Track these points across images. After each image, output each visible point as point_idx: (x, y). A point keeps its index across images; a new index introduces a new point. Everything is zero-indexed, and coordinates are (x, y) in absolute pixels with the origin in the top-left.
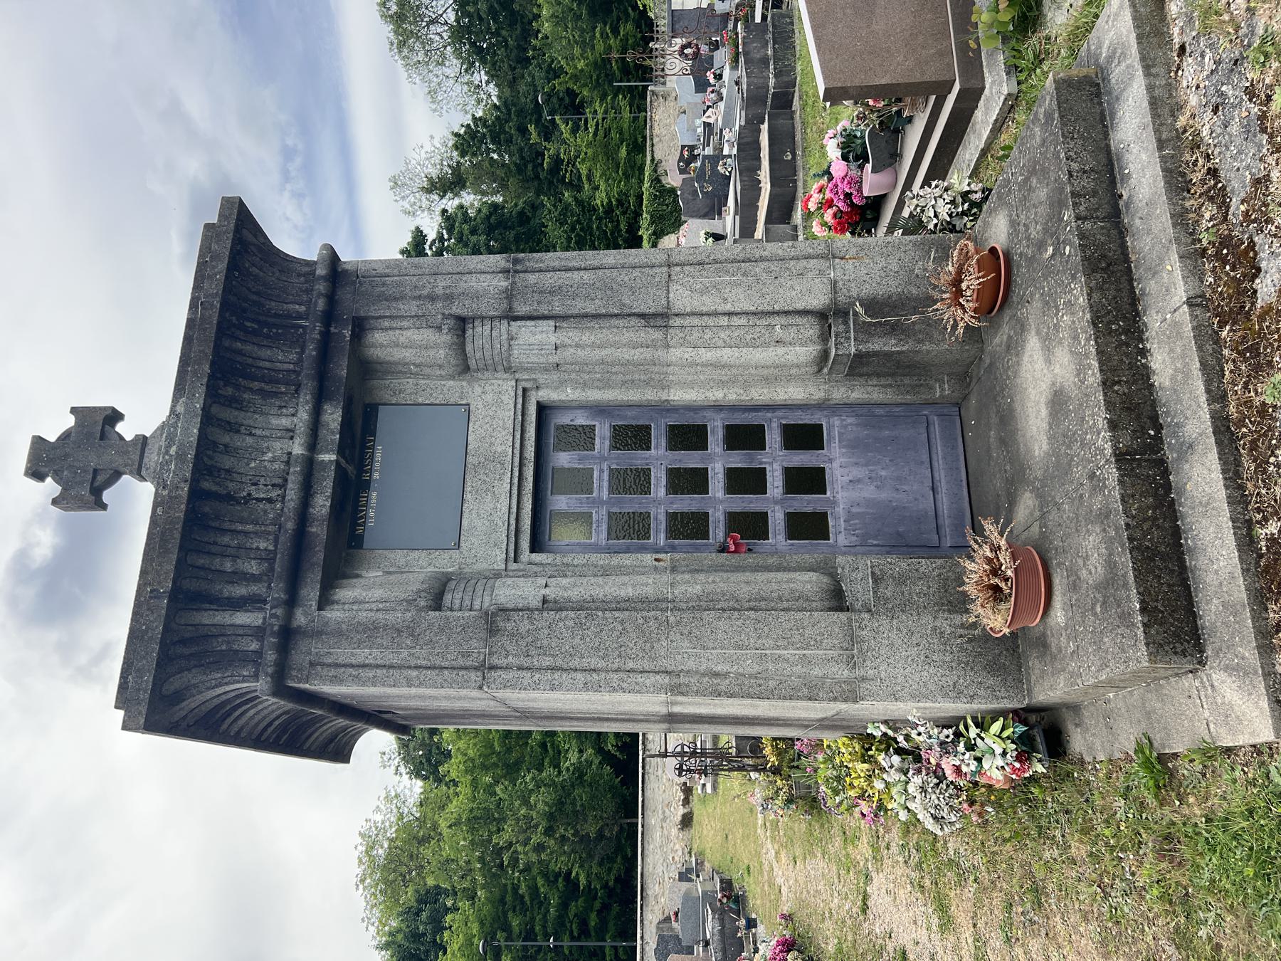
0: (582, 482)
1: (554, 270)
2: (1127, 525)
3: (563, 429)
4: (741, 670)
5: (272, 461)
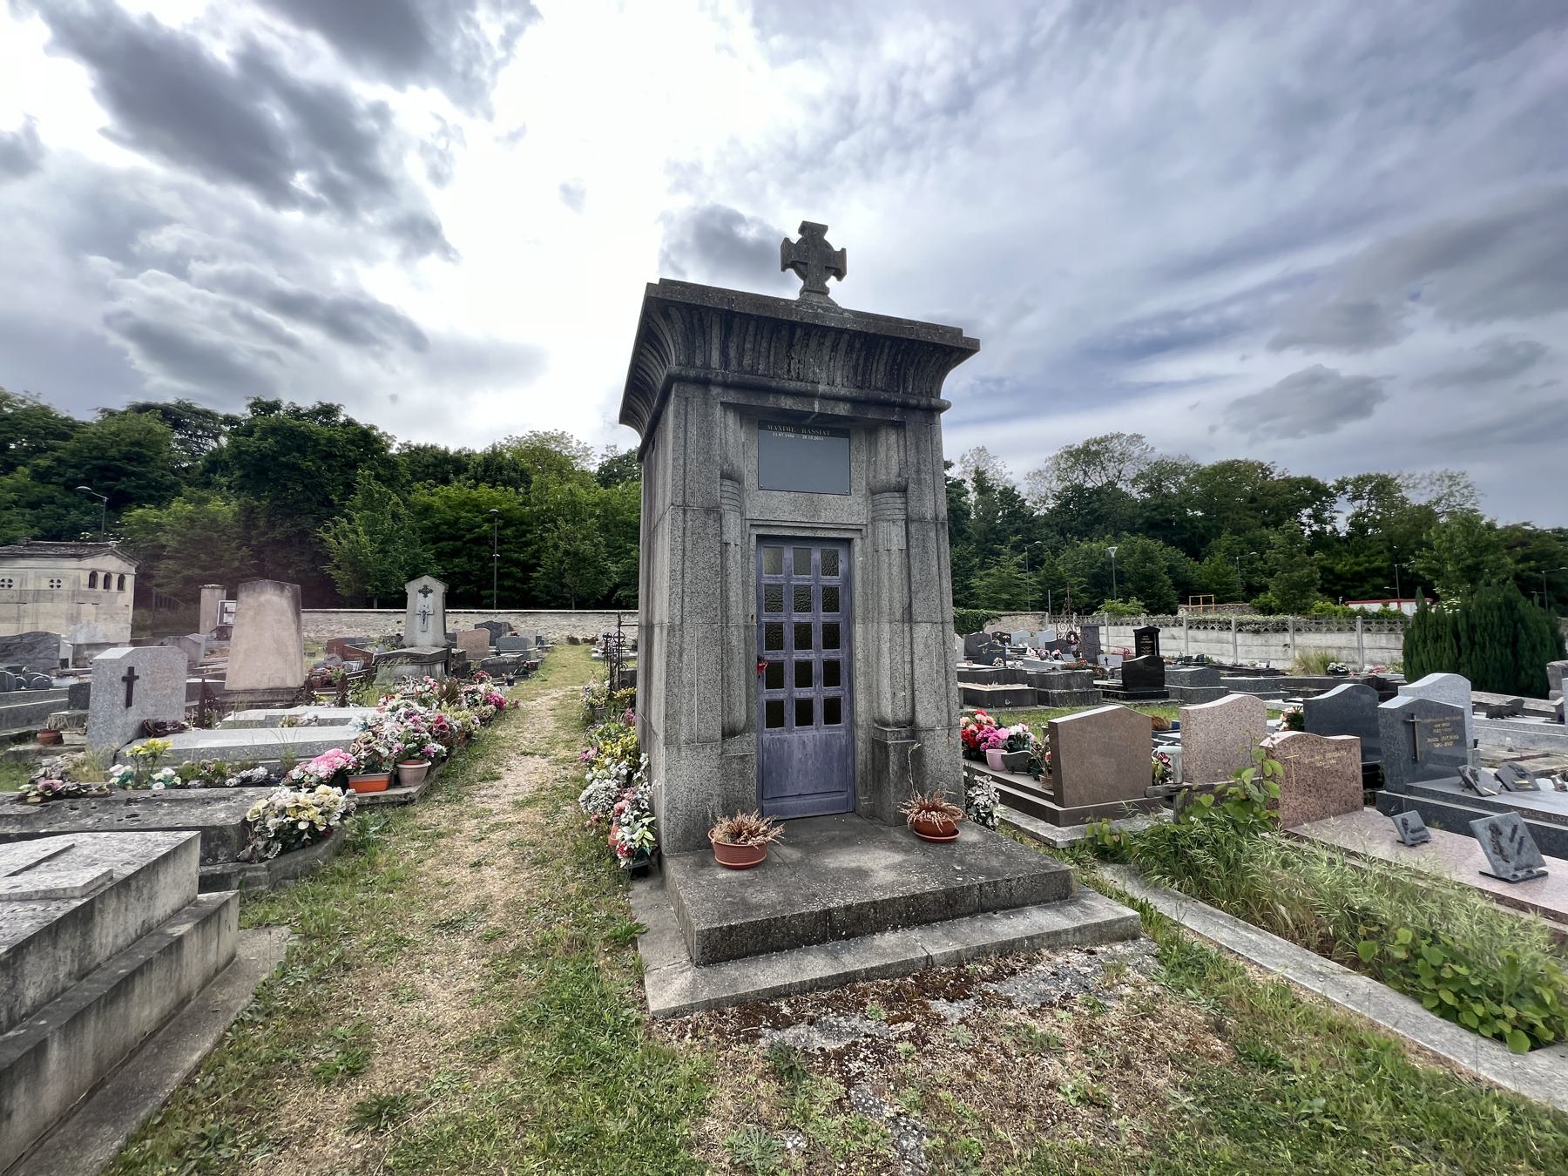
0: (802, 566)
3: (836, 555)
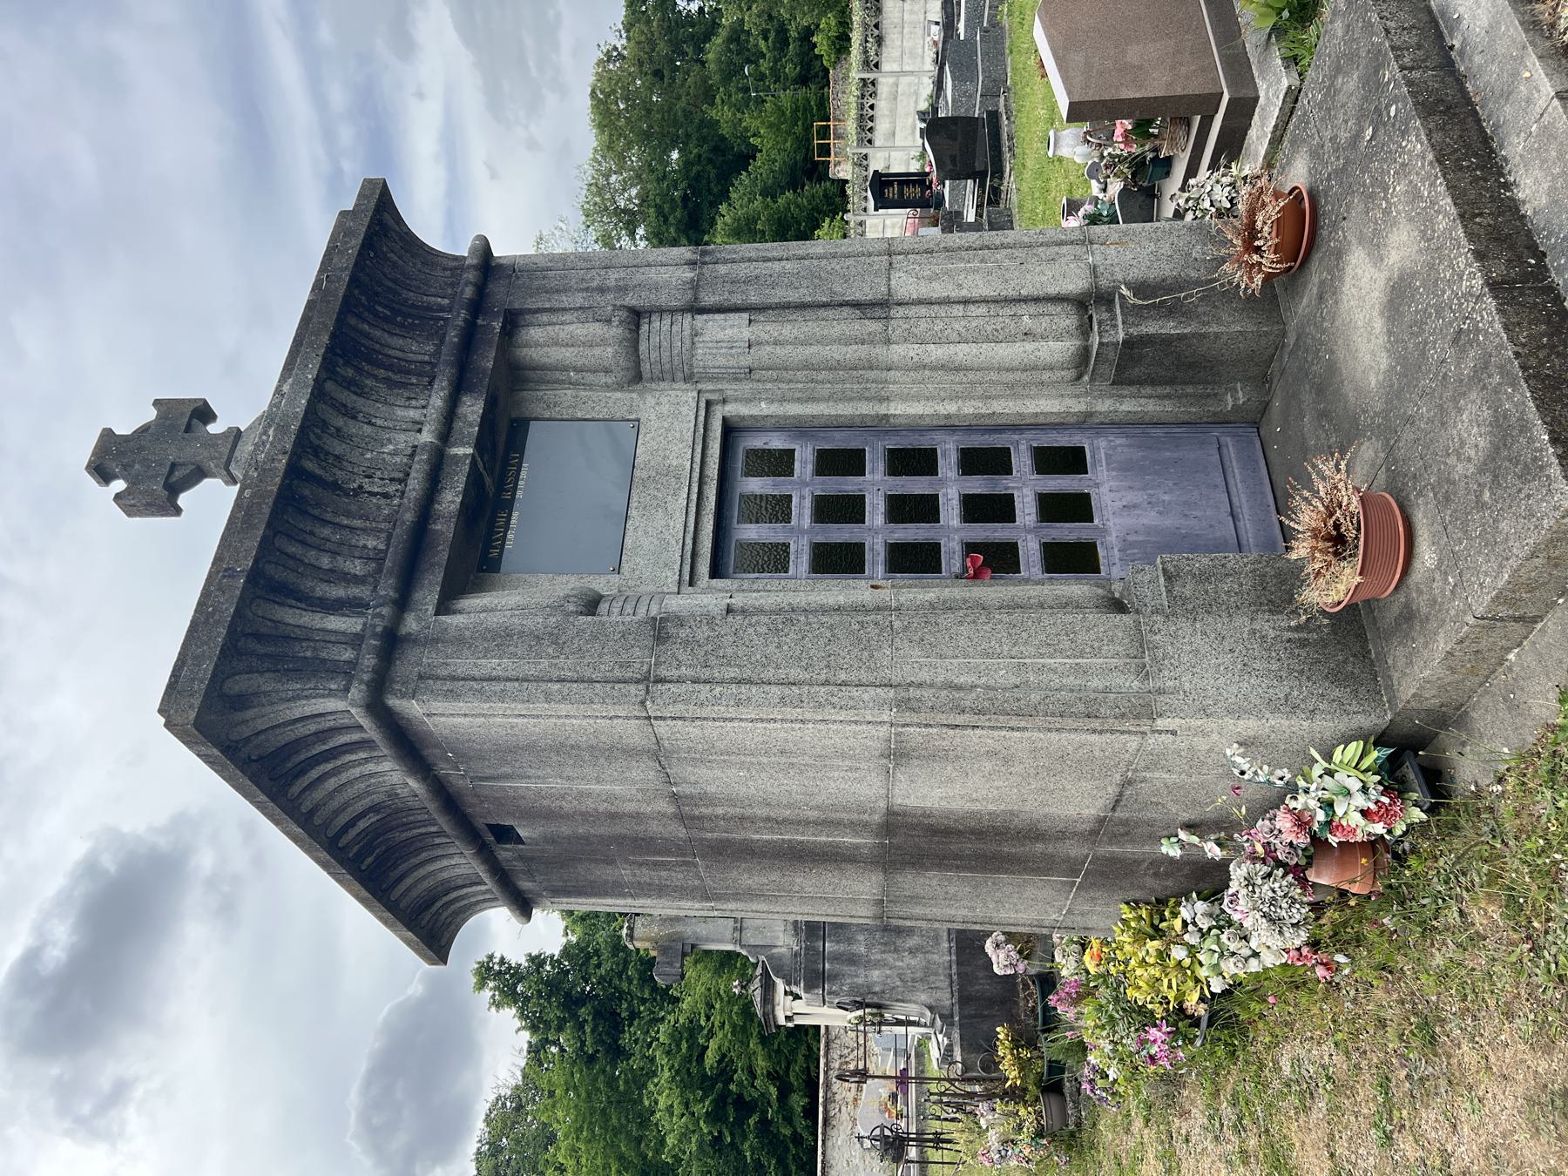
0: (779, 509)
1: (750, 260)
2: (1517, 355)
3: (748, 499)
4: (991, 682)
5: (394, 453)
